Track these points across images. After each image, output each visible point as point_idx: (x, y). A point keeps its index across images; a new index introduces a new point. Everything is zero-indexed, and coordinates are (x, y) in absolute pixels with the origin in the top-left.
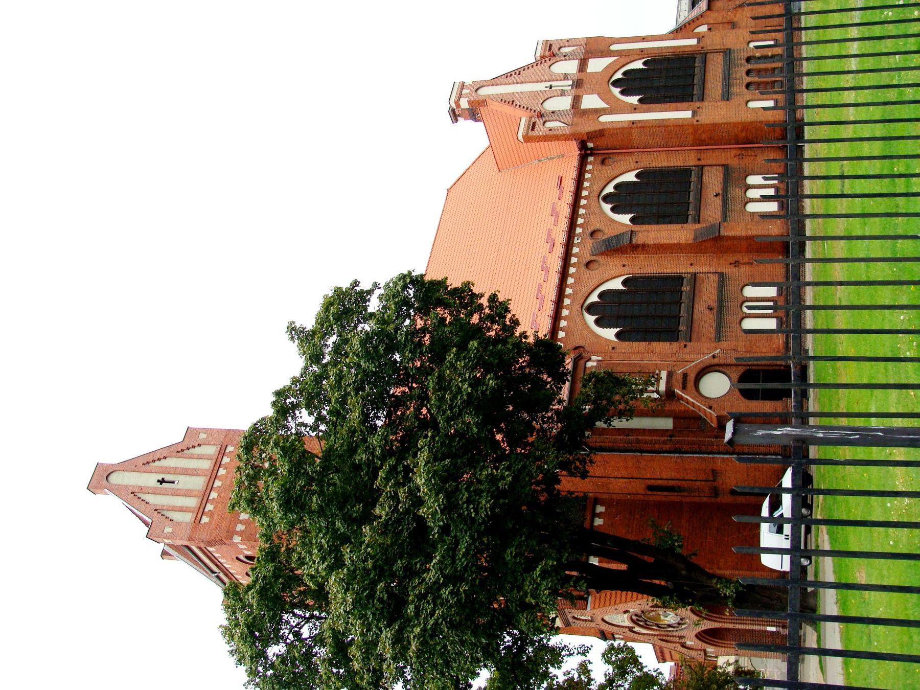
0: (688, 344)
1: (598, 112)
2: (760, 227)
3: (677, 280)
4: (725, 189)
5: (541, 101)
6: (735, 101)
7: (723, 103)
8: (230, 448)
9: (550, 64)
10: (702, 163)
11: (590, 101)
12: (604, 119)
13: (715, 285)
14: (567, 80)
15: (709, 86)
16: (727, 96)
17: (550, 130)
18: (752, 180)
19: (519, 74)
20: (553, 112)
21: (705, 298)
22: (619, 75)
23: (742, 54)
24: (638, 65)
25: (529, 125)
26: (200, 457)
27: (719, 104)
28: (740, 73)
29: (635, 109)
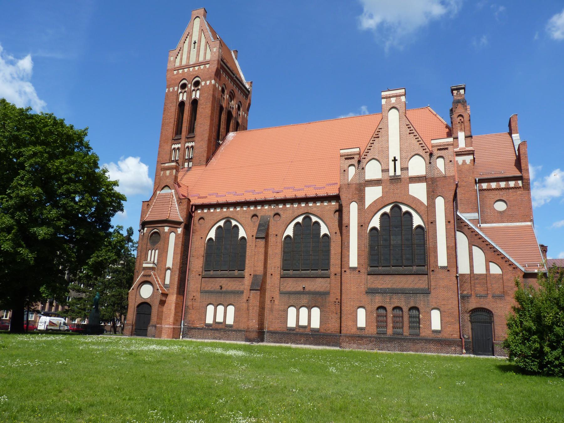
0: (201, 277)
1: (361, 200)
2: (254, 315)
3: (242, 268)
4: (309, 293)
5: (376, 157)
6: (366, 299)
7: (363, 288)
8: (208, 66)
9: (421, 154)
10: (332, 277)
12: (354, 207)
13: (237, 289)
14: (401, 170)
15: (388, 278)
16: (371, 292)
17: (344, 171)
18: (316, 312)
19: (410, 133)
20: (363, 168)
21: (229, 284)
22: (404, 209)
23: (422, 303)
24: (417, 221)
25: (351, 155)
26: (205, 54)
27: (363, 287)
28: (398, 301)
29: (361, 226)
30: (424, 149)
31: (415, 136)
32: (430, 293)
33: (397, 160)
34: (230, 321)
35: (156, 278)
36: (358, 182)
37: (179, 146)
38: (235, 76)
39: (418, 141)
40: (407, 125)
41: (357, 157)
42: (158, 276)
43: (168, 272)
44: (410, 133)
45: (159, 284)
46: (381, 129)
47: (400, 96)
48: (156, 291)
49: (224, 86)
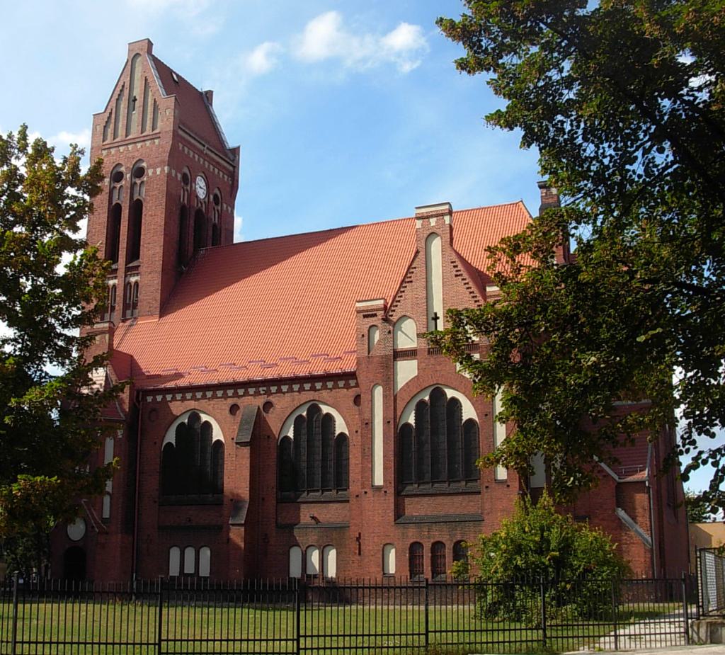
1: (388, 379)
5: (408, 314)
8: (157, 141)
10: (353, 500)
11: (406, 371)
12: (379, 392)
17: (363, 336)
19: (456, 276)
22: (450, 393)
25: (372, 310)
29: (386, 422)
30: (476, 301)
31: (463, 279)
32: (483, 520)
33: (438, 318)
34: (205, 571)
35: (90, 510)
36: (383, 353)
37: (115, 281)
38: (205, 148)
39: (468, 288)
40: (452, 262)
41: (381, 314)
42: (93, 506)
43: (107, 500)
44: (456, 276)
45: (94, 519)
46: (415, 268)
47: (443, 215)
48: (90, 529)
49: (186, 170)
